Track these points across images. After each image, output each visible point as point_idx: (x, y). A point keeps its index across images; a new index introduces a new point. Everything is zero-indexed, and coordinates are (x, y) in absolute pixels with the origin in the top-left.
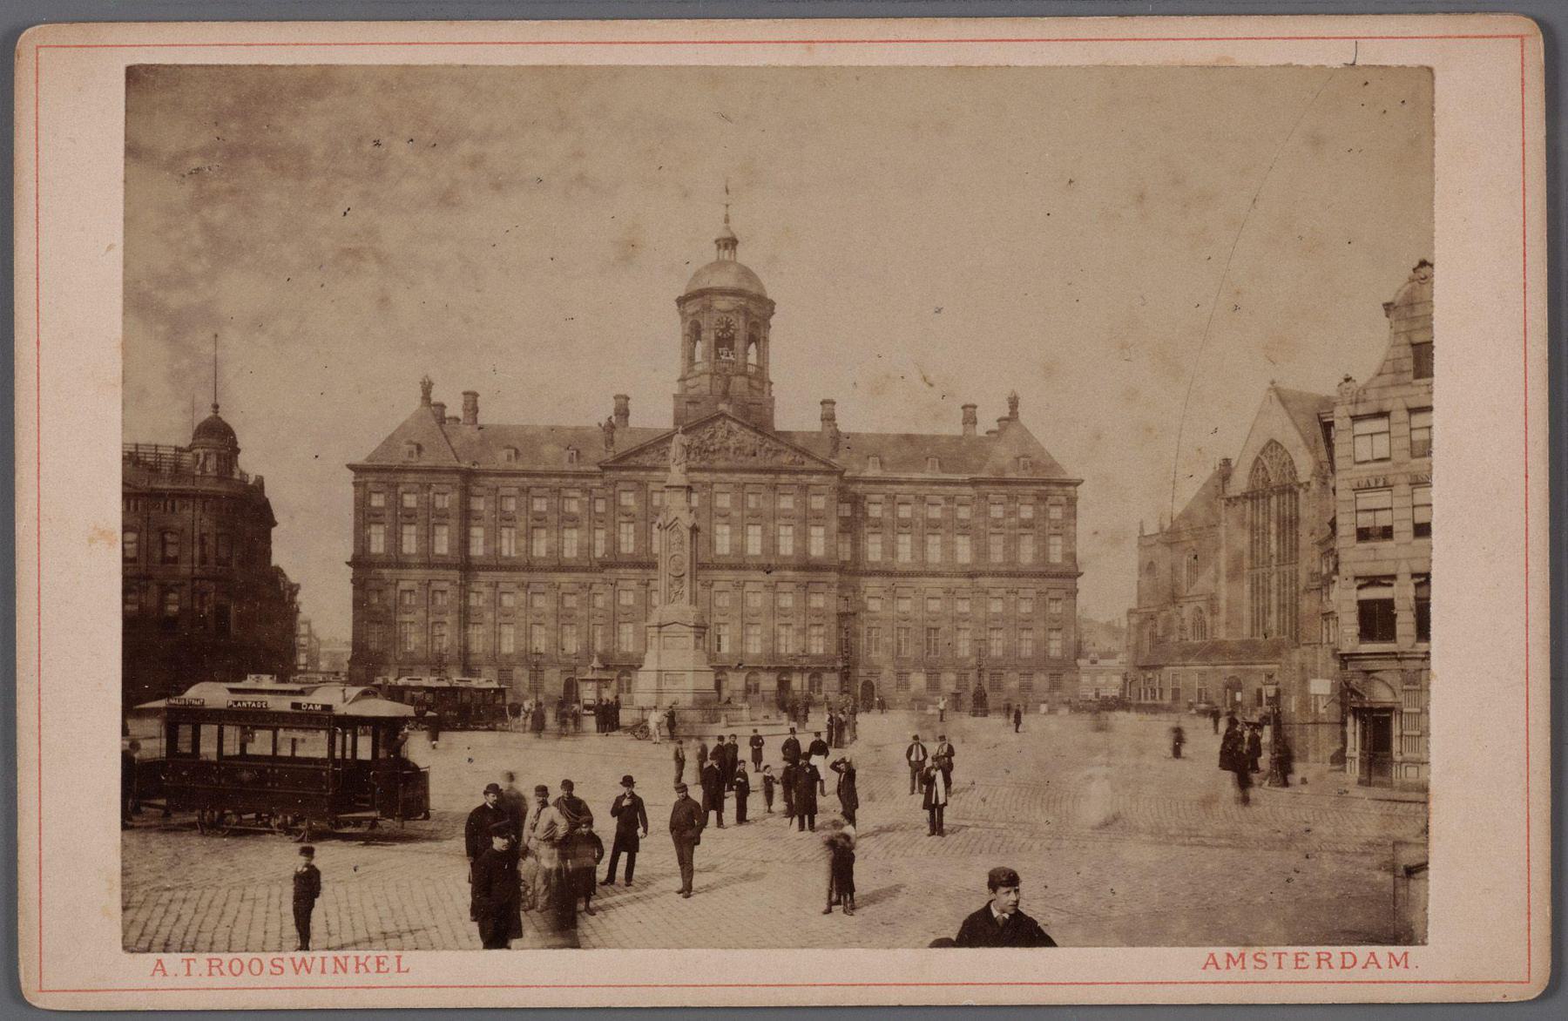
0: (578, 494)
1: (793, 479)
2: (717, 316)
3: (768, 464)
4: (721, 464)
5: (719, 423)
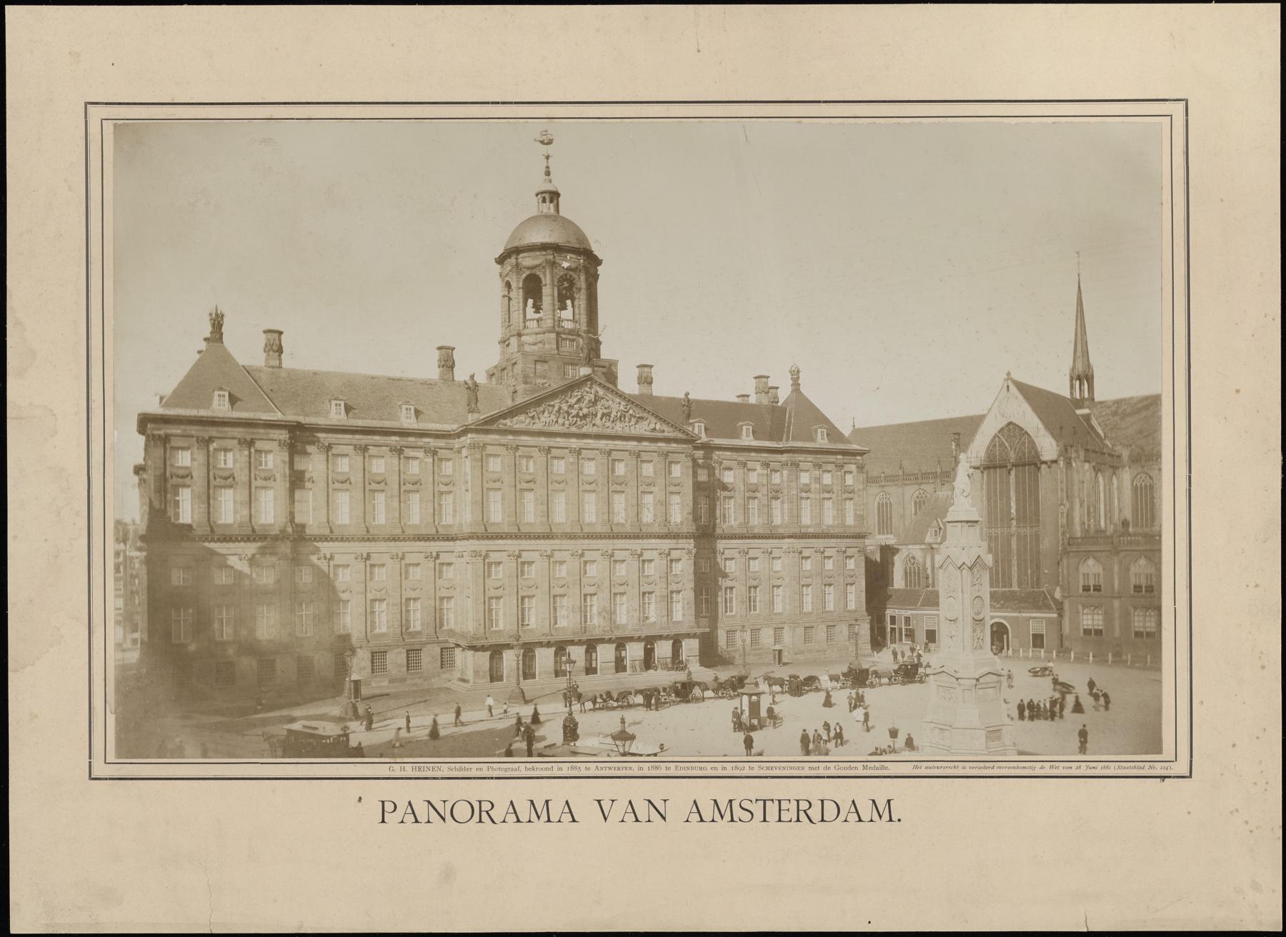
0: (420, 454)
1: (653, 446)
4: (588, 429)
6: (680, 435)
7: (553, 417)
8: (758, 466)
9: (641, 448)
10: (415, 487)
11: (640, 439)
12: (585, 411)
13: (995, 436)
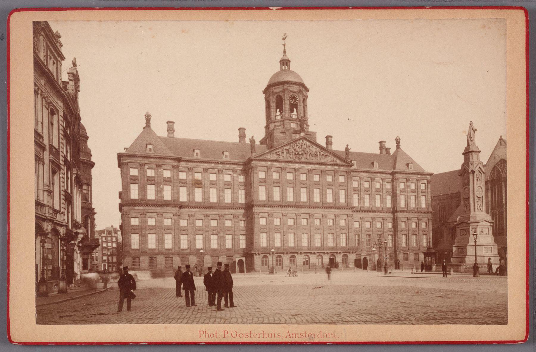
0: (231, 173)
2: (291, 94)
3: (323, 161)
4: (303, 160)
5: (301, 141)
6: (344, 163)
7: (288, 155)
8: (381, 181)
9: (326, 169)
10: (229, 187)
11: (326, 164)
12: (302, 152)
13: (495, 166)
